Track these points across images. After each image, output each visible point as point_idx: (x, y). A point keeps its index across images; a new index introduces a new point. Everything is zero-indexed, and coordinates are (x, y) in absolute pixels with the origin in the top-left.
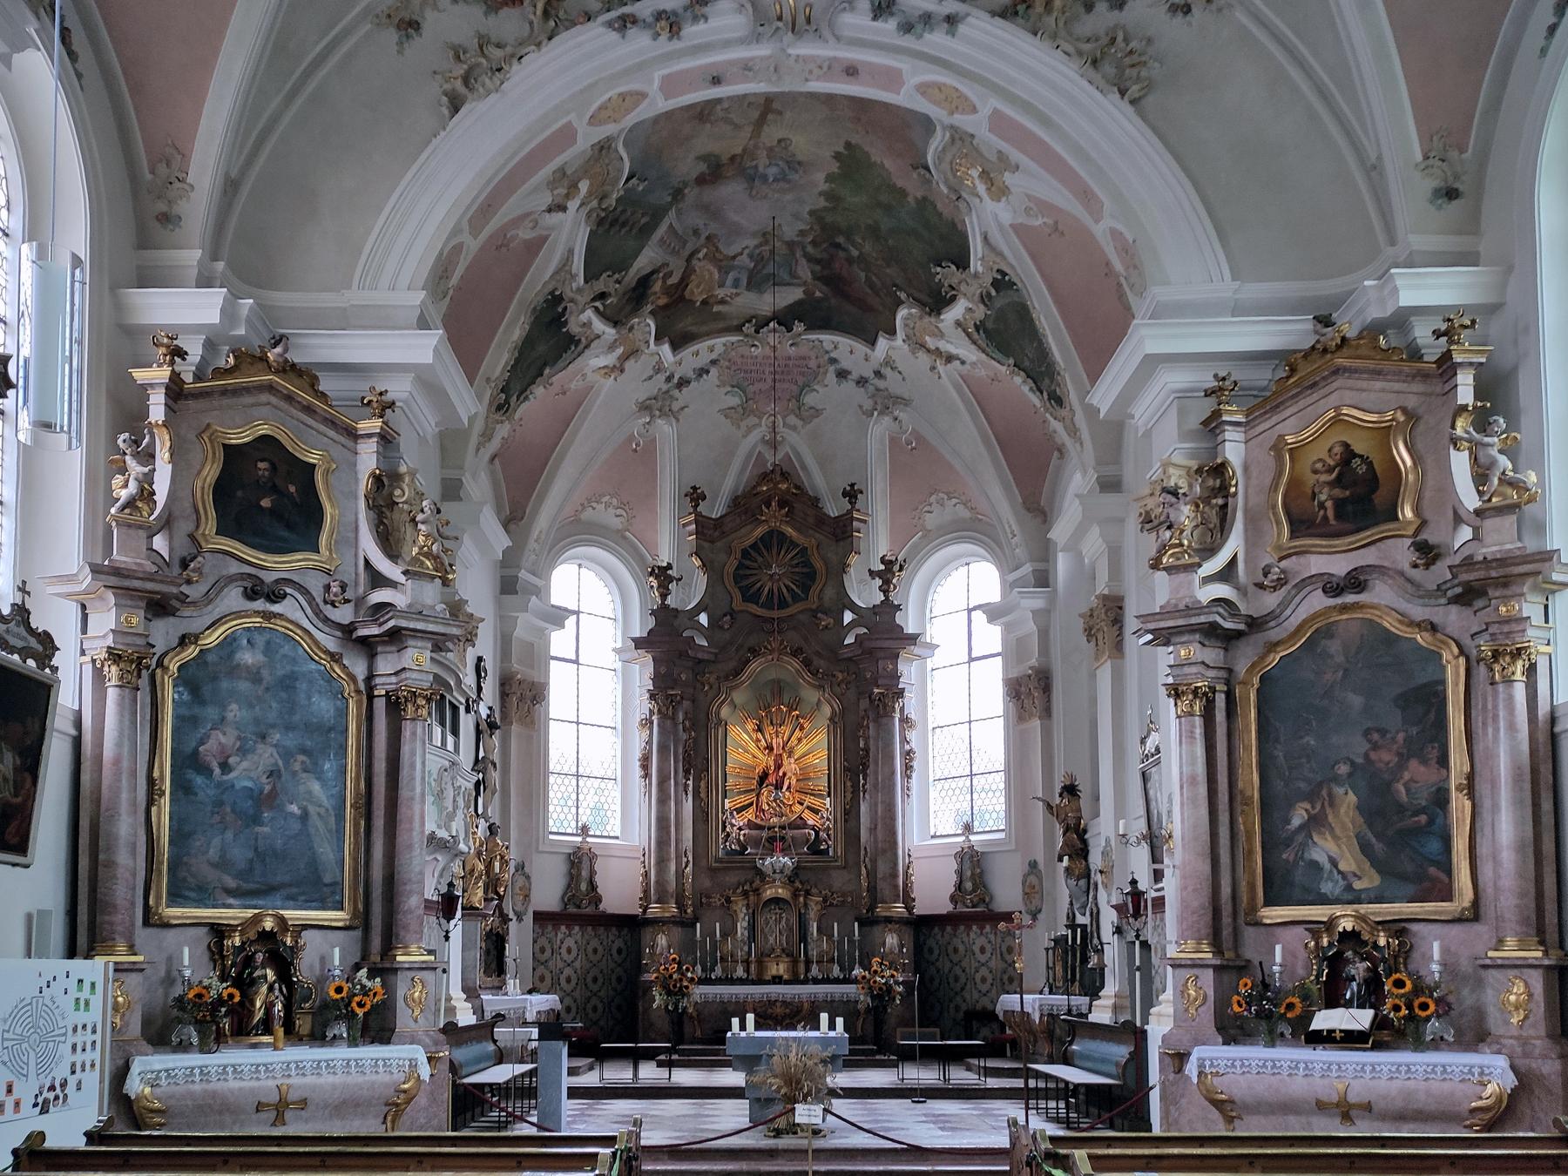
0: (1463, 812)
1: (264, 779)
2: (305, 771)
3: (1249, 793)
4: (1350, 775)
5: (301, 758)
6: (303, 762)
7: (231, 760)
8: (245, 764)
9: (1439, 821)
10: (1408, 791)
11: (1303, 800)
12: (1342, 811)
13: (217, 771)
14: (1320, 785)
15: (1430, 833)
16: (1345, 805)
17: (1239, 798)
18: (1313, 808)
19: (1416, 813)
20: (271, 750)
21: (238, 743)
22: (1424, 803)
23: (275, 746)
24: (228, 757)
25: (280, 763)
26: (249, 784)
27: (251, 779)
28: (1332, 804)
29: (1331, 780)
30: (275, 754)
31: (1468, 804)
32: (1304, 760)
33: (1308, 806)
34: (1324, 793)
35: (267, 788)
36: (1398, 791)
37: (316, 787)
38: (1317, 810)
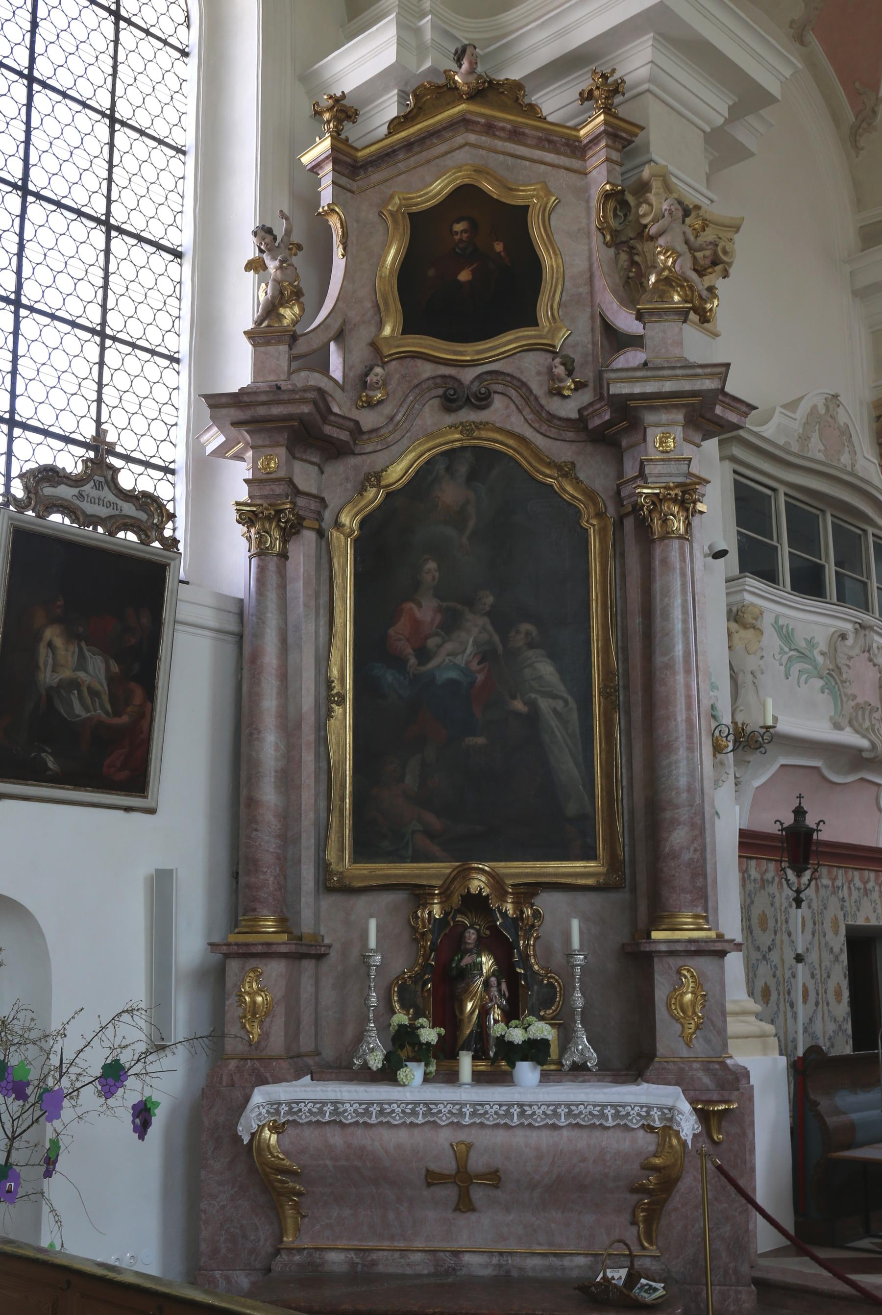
1: (474, 666)
2: (531, 646)
5: (526, 627)
6: (528, 634)
7: (432, 643)
8: (449, 647)
13: (413, 661)
20: (484, 621)
21: (439, 617)
23: (488, 614)
24: (426, 638)
25: (496, 638)
26: (453, 674)
27: (456, 666)
30: (490, 628)
35: (480, 677)
37: (547, 669)
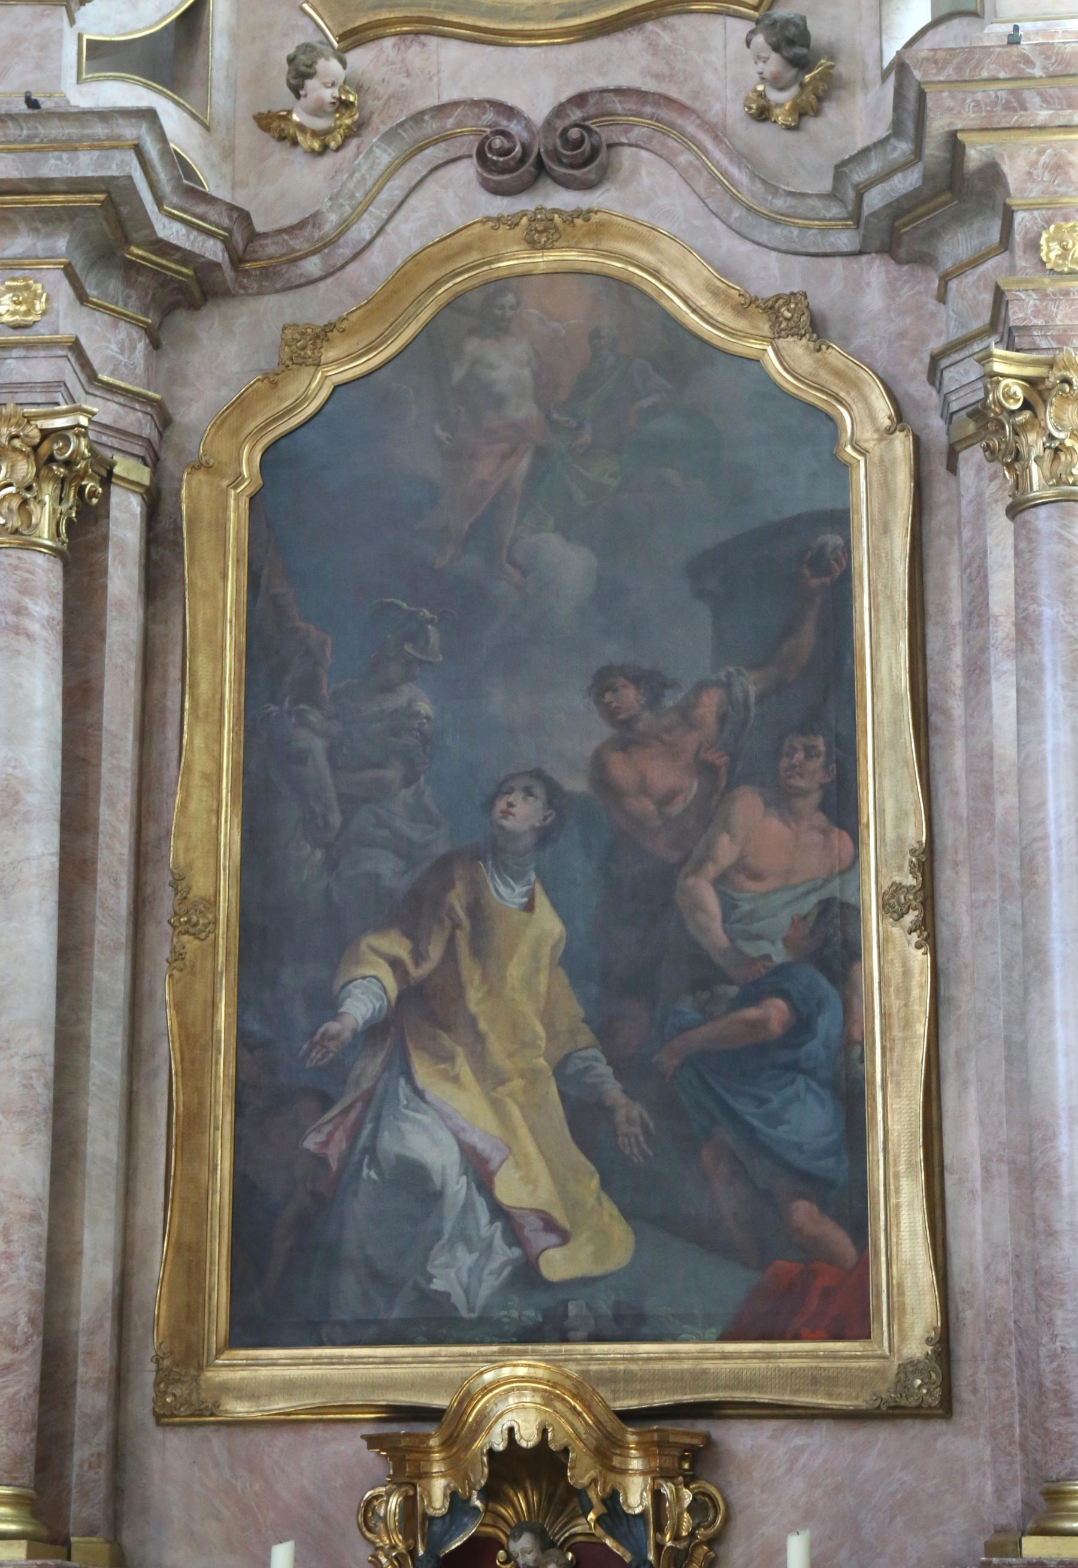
0: (905, 991)
3: (200, 886)
4: (544, 836)
9: (827, 1024)
10: (729, 906)
11: (380, 928)
12: (515, 971)
14: (444, 866)
15: (793, 1067)
16: (524, 950)
17: (165, 904)
18: (418, 956)
19: (753, 995)
22: (779, 955)
28: (480, 949)
29: (476, 855)
31: (920, 960)
32: (393, 773)
33: (397, 945)
34: (457, 900)
36: (698, 906)
38: (427, 968)
